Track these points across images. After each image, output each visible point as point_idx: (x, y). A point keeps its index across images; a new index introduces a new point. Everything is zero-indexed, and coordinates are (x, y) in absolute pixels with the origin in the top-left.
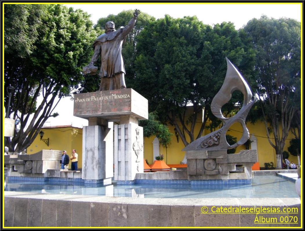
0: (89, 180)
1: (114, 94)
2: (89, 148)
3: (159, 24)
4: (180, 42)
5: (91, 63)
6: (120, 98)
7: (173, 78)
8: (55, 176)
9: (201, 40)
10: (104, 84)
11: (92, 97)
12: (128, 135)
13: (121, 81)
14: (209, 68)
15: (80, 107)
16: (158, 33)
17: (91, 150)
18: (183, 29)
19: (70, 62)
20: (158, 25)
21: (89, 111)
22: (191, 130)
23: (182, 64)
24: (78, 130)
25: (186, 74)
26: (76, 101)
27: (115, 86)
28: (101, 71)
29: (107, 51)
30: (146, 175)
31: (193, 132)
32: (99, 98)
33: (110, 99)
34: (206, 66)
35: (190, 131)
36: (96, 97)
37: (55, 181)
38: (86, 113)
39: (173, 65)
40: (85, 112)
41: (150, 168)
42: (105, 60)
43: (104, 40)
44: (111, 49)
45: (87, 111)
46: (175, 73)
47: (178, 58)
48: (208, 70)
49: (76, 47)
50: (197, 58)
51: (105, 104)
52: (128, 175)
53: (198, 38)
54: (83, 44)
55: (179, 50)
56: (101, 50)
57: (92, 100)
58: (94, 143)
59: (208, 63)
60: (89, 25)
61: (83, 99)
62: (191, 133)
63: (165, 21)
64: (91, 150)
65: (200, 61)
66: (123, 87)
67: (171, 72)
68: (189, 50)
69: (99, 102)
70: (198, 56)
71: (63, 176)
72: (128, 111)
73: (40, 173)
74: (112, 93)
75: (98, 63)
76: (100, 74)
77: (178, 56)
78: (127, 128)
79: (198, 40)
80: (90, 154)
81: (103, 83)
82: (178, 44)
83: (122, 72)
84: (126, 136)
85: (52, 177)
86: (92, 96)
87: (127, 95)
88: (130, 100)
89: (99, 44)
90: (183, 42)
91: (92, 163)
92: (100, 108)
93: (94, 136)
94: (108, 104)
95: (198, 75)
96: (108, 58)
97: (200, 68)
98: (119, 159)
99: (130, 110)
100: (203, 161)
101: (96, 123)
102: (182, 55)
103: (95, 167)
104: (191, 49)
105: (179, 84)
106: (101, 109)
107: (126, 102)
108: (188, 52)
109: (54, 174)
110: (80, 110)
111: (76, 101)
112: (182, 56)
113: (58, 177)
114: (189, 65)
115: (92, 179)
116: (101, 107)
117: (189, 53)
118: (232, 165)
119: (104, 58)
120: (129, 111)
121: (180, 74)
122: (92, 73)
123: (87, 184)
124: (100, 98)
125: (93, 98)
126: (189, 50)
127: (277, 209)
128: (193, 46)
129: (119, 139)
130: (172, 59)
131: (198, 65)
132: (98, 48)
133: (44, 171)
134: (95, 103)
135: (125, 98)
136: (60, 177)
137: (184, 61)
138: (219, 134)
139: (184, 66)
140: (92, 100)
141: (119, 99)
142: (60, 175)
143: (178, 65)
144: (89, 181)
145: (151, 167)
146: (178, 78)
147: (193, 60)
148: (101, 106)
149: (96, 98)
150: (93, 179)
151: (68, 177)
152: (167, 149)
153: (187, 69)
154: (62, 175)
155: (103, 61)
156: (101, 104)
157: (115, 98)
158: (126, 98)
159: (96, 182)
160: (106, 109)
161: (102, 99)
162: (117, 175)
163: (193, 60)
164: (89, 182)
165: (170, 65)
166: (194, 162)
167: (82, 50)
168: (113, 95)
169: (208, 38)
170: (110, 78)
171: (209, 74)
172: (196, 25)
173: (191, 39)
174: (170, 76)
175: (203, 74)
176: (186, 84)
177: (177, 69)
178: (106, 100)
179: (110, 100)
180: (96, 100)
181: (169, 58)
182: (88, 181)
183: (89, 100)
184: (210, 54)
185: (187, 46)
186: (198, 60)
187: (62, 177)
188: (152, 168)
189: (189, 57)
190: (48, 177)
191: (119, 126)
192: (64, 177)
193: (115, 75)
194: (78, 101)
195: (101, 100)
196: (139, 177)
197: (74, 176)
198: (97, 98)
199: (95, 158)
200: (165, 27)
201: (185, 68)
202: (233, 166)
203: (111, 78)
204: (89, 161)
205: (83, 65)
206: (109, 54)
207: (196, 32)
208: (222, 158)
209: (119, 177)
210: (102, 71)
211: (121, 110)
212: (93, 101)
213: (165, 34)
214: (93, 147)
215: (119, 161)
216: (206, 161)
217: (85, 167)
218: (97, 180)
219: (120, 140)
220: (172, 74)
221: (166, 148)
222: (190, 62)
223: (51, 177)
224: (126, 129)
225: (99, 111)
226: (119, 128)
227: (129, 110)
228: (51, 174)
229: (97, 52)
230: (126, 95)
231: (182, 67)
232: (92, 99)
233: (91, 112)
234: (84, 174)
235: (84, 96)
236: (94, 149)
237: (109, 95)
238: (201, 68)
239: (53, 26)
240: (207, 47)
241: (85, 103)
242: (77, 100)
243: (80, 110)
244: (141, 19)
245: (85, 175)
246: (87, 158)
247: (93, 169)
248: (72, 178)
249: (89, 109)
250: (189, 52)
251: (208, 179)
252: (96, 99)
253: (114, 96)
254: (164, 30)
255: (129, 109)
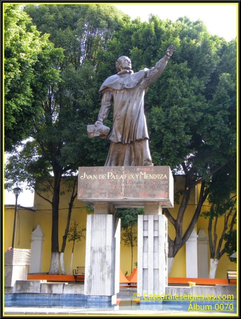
0: (95, 297)
1: (143, 172)
2: (96, 248)
3: (143, 33)
4: (179, 71)
5: (100, 121)
6: (152, 178)
7: (165, 131)
8: (31, 291)
9: (214, 69)
10: (116, 153)
11: (108, 173)
12: (158, 230)
13: (144, 151)
14: (224, 118)
15: (89, 187)
16: (140, 50)
17: (100, 250)
18: (185, 47)
20: (140, 35)
21: (105, 194)
22: (178, 217)
23: (183, 109)
25: (186, 125)
26: (82, 176)
27: (133, 156)
28: (113, 133)
29: (123, 105)
30: (181, 290)
31: (181, 221)
32: (120, 176)
33: (137, 178)
34: (220, 115)
35: (176, 219)
36: (115, 173)
37: (29, 299)
38: (99, 196)
39: (165, 107)
40: (97, 194)
41: (129, 282)
42: (119, 117)
43: (119, 87)
44: (129, 102)
45: (101, 194)
46: (168, 122)
47: (175, 97)
48: (223, 122)
50: (206, 100)
51: (129, 185)
52: (158, 289)
53: (210, 64)
54: (19, 61)
55: (178, 84)
56: (112, 100)
57: (108, 178)
58: (106, 240)
59: (224, 108)
61: (94, 176)
62: (179, 222)
63: (153, 29)
64: (100, 250)
65: (211, 105)
66: (148, 160)
67: (163, 121)
68: (193, 85)
69: (119, 181)
70: (209, 97)
71: (45, 290)
72: (165, 197)
74: (140, 171)
75: (110, 120)
76: (112, 139)
77: (174, 95)
78: (158, 221)
79: (209, 68)
80: (98, 256)
81: (114, 151)
82: (176, 73)
83: (146, 138)
84: (156, 232)
85: (25, 292)
86: (109, 171)
87: (164, 175)
88: (167, 182)
89: (110, 92)
90: (184, 71)
91: (102, 270)
92: (122, 191)
93: (105, 230)
94: (134, 185)
95: (205, 128)
96: (126, 115)
97: (210, 116)
98: (144, 265)
101: (106, 210)
102: (182, 92)
103: (106, 276)
104: (197, 83)
105: (175, 141)
106: (123, 193)
107: (163, 185)
108: (192, 89)
109: (28, 289)
110: (89, 191)
111: (82, 176)
112: (183, 95)
113: (35, 292)
114: (193, 111)
115: (101, 295)
116: (123, 189)
117: (194, 90)
119: (118, 115)
120: (166, 198)
121: (177, 125)
122: (102, 135)
123: (91, 302)
124: (122, 176)
125: (110, 175)
126: (193, 85)
128: (199, 77)
129: (146, 235)
130: (165, 97)
131: (206, 111)
132: (107, 98)
134: (115, 182)
135: (160, 179)
136: (39, 292)
137: (186, 103)
139: (185, 112)
140: (108, 178)
141: (151, 179)
142: (39, 290)
143: (176, 110)
144: (95, 298)
145: (129, 281)
146: (174, 132)
147: (200, 103)
148: (122, 188)
149: (115, 175)
150: (103, 295)
151: (54, 292)
152: (133, 247)
153: (188, 117)
154: (42, 289)
155: (117, 118)
156: (123, 185)
157: (145, 178)
158: (163, 180)
159: (106, 300)
160: (132, 193)
161: (125, 178)
162: (142, 289)
163: (200, 103)
164: (94, 300)
165: (161, 109)
168: (141, 172)
169: (225, 64)
170: (126, 144)
171: (224, 128)
172: (208, 42)
173: (197, 66)
174: (160, 127)
175: (214, 127)
176: (186, 142)
177: (172, 116)
178: (130, 180)
179: (137, 181)
180: (115, 178)
181: (158, 95)
182: (93, 298)
183: (103, 177)
184: (228, 94)
185: (190, 77)
186: (207, 102)
187: (42, 292)
188: (131, 281)
189: (194, 97)
190: (17, 292)
191: (146, 217)
192: (47, 292)
193: (135, 141)
194: (86, 177)
195: (123, 178)
196: (170, 292)
197: (64, 290)
198: (117, 175)
199: (107, 263)
200: (151, 40)
201: (186, 116)
203: (127, 145)
204: (97, 267)
205: (16, 97)
206: (127, 110)
207: (208, 55)
209: (144, 292)
210: (114, 134)
211: (154, 195)
212: (110, 179)
213: (152, 53)
214: (103, 246)
215: (145, 268)
217: (89, 276)
218: (108, 296)
219: (147, 237)
220: (163, 124)
221: (131, 247)
222: (194, 106)
223: (23, 293)
225: (119, 194)
226: (145, 220)
227: (166, 196)
228: (22, 288)
229: (108, 104)
230: (162, 175)
231: (181, 114)
232: (108, 176)
233: (107, 196)
234: (88, 286)
235: (95, 170)
236: (105, 249)
237: (136, 172)
238: (212, 117)
240: (225, 83)
241: (96, 181)
242: (84, 176)
243: (89, 191)
244: (106, 16)
245: (90, 289)
246: (93, 262)
247: (103, 279)
248: (60, 294)
249: (104, 191)
250: (193, 88)
252: (116, 178)
253: (143, 175)
254: (150, 44)
255: (166, 195)
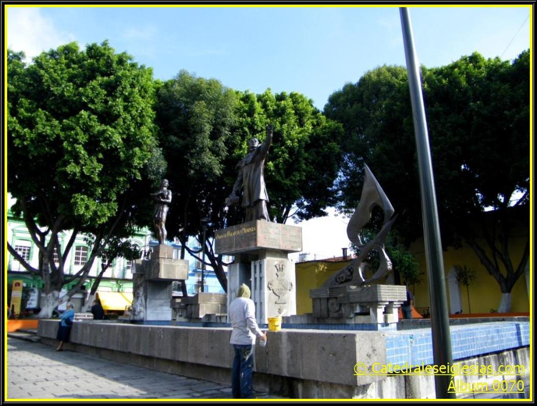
19: (272, 175)
24: (326, 264)
49: (278, 153)
54: (287, 147)
60: (303, 114)
73: (197, 317)
94: (240, 239)
99: (256, 245)
100: (326, 301)
118: (354, 305)
127: (438, 370)
133: (201, 316)
134: (230, 238)
136: (215, 321)
138: (352, 266)
152: (469, 286)
166: (318, 301)
167: (287, 155)
202: (356, 306)
208: (343, 297)
216: (331, 301)
224: (261, 266)
239: (246, 132)
251: (334, 323)
